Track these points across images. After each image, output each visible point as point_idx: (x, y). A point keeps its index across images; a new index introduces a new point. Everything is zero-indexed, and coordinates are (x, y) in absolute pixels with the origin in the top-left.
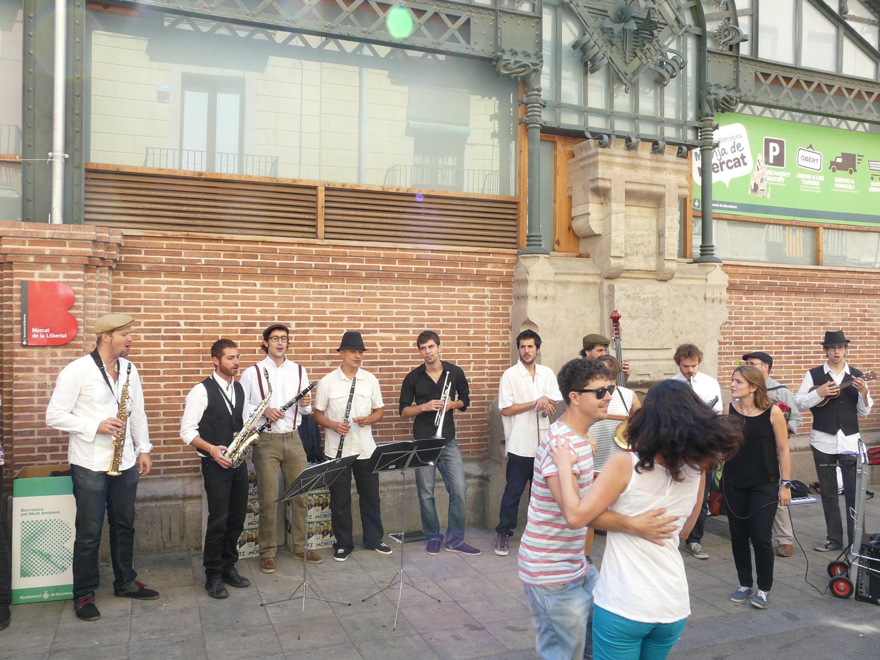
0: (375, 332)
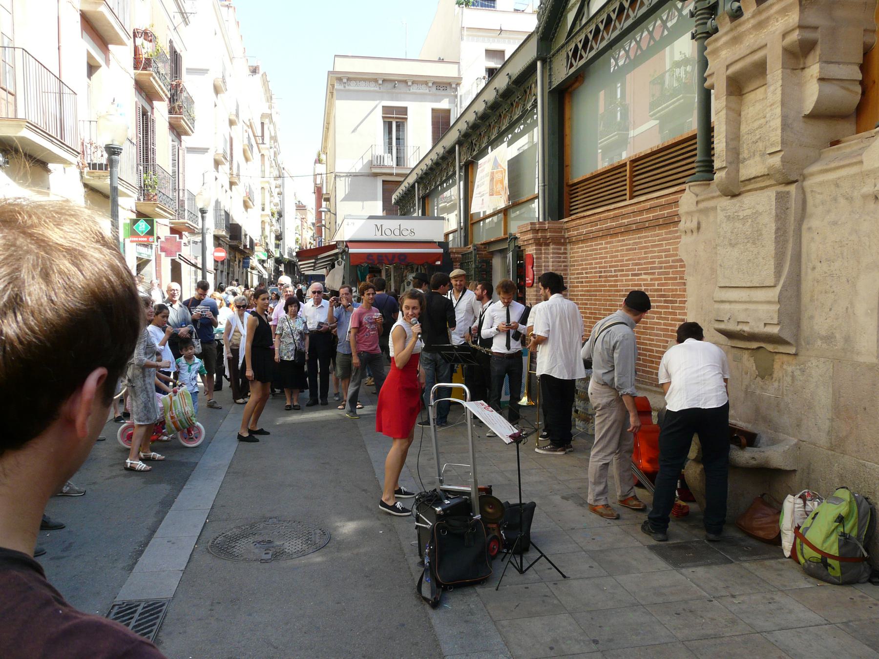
0: (641, 274)
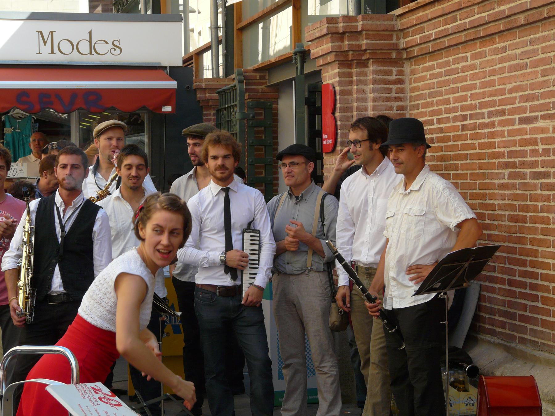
0: (535, 119)
